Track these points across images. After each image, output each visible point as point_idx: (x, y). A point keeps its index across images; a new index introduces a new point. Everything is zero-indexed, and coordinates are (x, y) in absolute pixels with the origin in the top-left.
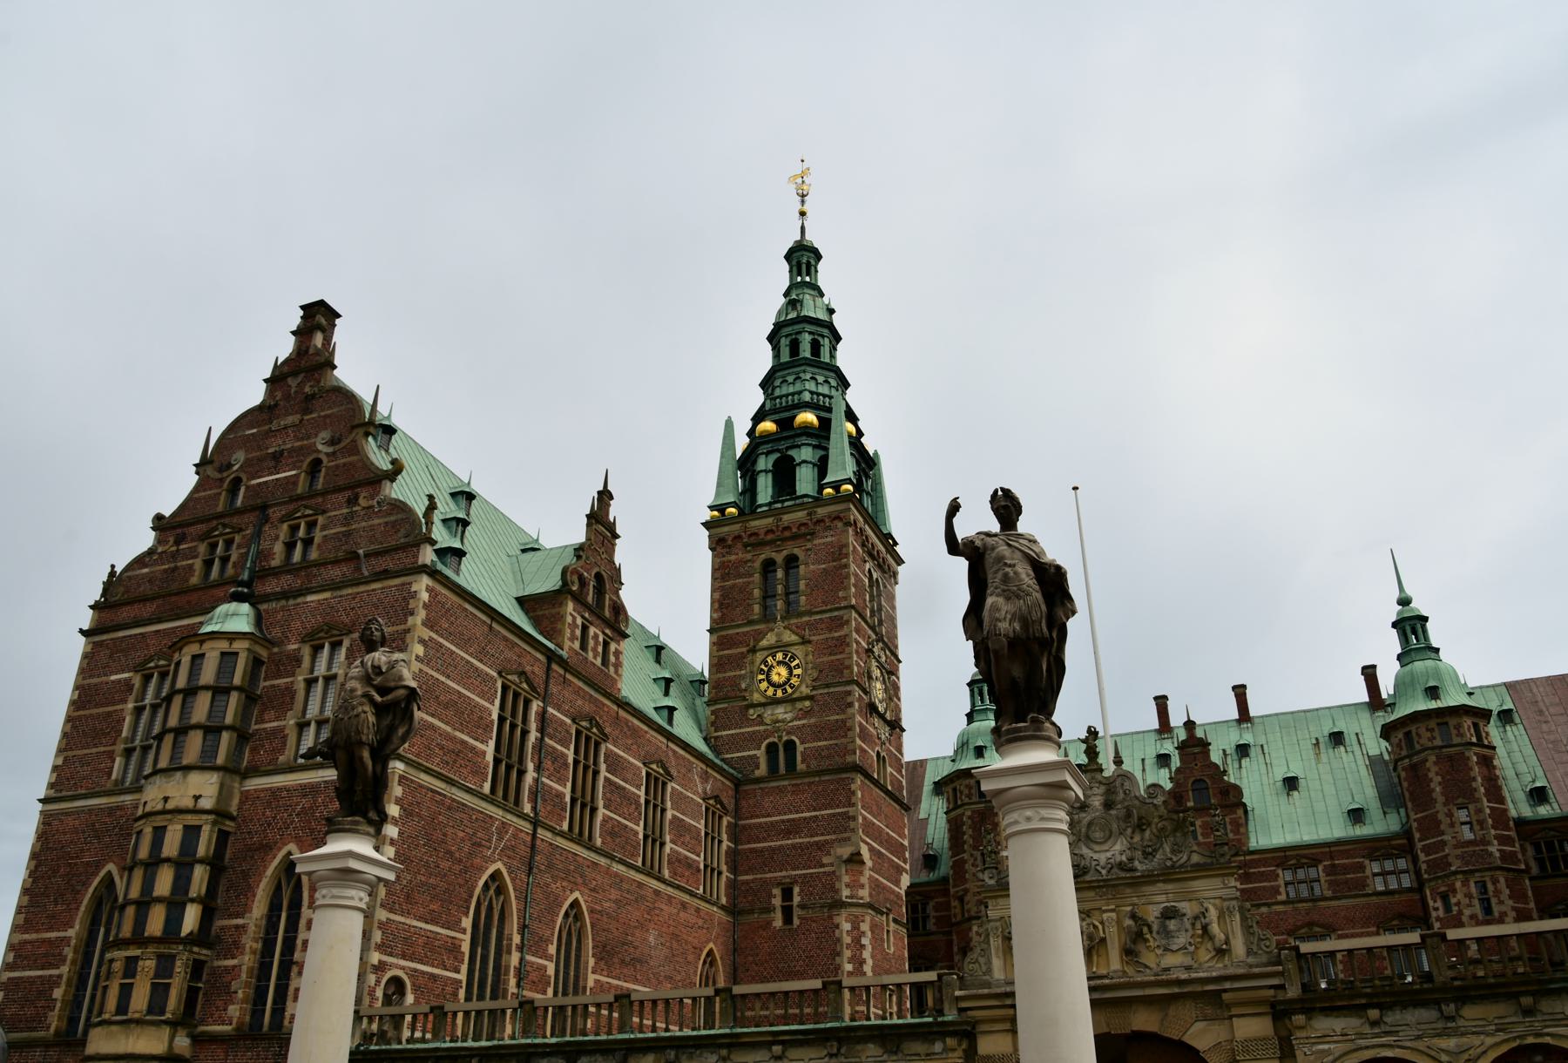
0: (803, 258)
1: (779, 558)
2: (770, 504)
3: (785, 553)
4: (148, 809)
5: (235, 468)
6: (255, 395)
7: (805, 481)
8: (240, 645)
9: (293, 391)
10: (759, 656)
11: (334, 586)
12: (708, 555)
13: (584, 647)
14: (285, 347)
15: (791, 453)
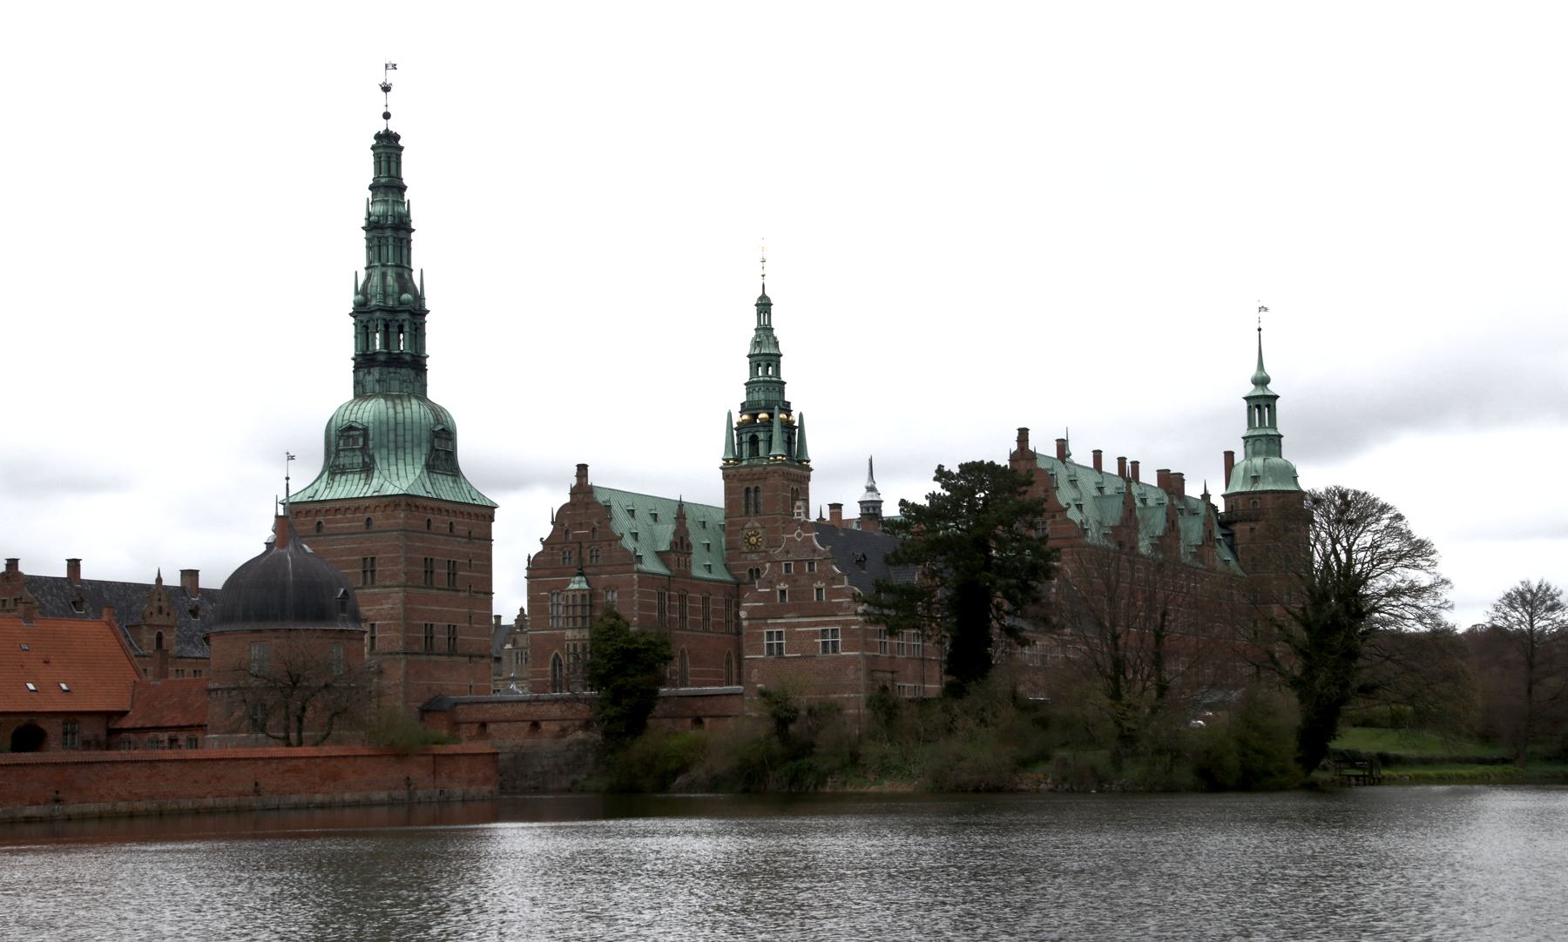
0: (764, 306)
1: (752, 488)
2: (748, 459)
3: (755, 485)
4: (570, 638)
5: (566, 525)
6: (567, 499)
7: (762, 446)
8: (586, 593)
9: (581, 499)
10: (746, 531)
11: (611, 573)
12: (723, 481)
13: (679, 566)
14: (574, 482)
15: (757, 434)
